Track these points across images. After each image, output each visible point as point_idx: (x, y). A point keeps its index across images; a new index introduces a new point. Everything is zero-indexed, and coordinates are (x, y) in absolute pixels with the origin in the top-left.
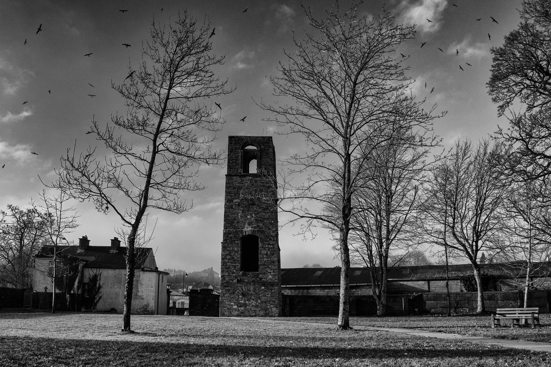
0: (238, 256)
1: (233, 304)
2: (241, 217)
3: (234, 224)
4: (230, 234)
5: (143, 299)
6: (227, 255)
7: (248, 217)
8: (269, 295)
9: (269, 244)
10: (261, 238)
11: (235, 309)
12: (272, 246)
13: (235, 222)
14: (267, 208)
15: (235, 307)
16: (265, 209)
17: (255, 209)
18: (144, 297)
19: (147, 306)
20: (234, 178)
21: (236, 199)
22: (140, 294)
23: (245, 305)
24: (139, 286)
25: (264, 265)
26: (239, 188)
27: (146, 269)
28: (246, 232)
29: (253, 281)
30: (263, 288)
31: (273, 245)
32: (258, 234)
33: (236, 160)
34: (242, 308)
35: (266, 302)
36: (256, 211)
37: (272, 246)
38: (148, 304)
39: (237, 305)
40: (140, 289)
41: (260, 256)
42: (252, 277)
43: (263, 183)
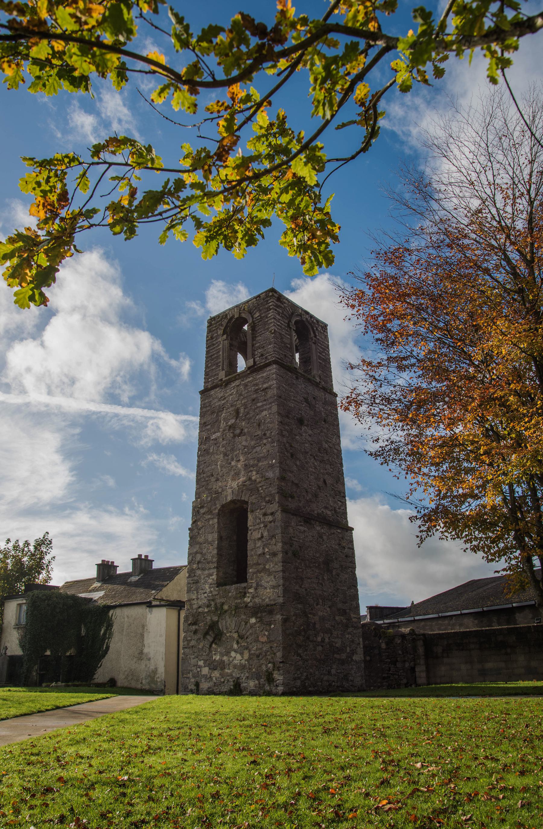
0: (212, 552)
1: (201, 663)
2: (221, 467)
3: (210, 487)
4: (202, 507)
5: (149, 659)
6: (196, 553)
7: (233, 463)
8: (264, 639)
9: (265, 515)
10: (252, 503)
11: (205, 676)
12: (270, 518)
13: (213, 479)
14: (265, 434)
15: (205, 671)
16: (261, 439)
17: (244, 443)
18: (151, 655)
19: (155, 671)
20: (212, 392)
21: (214, 433)
22: (146, 650)
23: (221, 666)
24: (145, 635)
25: (258, 564)
26: (221, 409)
27: (154, 603)
28: (226, 496)
29: (237, 607)
30: (253, 620)
31: (272, 514)
32: (245, 498)
33: (218, 357)
34: (216, 674)
35: (258, 656)
36: (245, 447)
37: (270, 518)
38: (156, 669)
39: (209, 666)
40: (146, 642)
41: (250, 545)
42: (236, 598)
43: (257, 385)
